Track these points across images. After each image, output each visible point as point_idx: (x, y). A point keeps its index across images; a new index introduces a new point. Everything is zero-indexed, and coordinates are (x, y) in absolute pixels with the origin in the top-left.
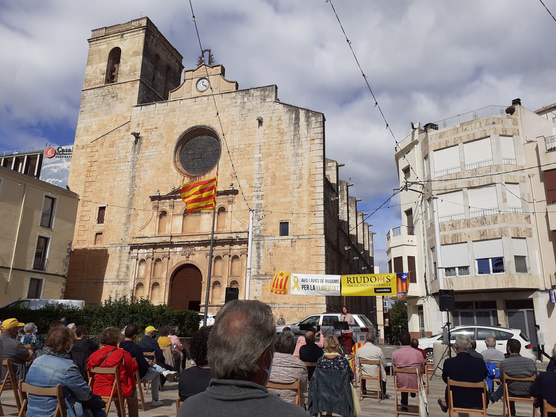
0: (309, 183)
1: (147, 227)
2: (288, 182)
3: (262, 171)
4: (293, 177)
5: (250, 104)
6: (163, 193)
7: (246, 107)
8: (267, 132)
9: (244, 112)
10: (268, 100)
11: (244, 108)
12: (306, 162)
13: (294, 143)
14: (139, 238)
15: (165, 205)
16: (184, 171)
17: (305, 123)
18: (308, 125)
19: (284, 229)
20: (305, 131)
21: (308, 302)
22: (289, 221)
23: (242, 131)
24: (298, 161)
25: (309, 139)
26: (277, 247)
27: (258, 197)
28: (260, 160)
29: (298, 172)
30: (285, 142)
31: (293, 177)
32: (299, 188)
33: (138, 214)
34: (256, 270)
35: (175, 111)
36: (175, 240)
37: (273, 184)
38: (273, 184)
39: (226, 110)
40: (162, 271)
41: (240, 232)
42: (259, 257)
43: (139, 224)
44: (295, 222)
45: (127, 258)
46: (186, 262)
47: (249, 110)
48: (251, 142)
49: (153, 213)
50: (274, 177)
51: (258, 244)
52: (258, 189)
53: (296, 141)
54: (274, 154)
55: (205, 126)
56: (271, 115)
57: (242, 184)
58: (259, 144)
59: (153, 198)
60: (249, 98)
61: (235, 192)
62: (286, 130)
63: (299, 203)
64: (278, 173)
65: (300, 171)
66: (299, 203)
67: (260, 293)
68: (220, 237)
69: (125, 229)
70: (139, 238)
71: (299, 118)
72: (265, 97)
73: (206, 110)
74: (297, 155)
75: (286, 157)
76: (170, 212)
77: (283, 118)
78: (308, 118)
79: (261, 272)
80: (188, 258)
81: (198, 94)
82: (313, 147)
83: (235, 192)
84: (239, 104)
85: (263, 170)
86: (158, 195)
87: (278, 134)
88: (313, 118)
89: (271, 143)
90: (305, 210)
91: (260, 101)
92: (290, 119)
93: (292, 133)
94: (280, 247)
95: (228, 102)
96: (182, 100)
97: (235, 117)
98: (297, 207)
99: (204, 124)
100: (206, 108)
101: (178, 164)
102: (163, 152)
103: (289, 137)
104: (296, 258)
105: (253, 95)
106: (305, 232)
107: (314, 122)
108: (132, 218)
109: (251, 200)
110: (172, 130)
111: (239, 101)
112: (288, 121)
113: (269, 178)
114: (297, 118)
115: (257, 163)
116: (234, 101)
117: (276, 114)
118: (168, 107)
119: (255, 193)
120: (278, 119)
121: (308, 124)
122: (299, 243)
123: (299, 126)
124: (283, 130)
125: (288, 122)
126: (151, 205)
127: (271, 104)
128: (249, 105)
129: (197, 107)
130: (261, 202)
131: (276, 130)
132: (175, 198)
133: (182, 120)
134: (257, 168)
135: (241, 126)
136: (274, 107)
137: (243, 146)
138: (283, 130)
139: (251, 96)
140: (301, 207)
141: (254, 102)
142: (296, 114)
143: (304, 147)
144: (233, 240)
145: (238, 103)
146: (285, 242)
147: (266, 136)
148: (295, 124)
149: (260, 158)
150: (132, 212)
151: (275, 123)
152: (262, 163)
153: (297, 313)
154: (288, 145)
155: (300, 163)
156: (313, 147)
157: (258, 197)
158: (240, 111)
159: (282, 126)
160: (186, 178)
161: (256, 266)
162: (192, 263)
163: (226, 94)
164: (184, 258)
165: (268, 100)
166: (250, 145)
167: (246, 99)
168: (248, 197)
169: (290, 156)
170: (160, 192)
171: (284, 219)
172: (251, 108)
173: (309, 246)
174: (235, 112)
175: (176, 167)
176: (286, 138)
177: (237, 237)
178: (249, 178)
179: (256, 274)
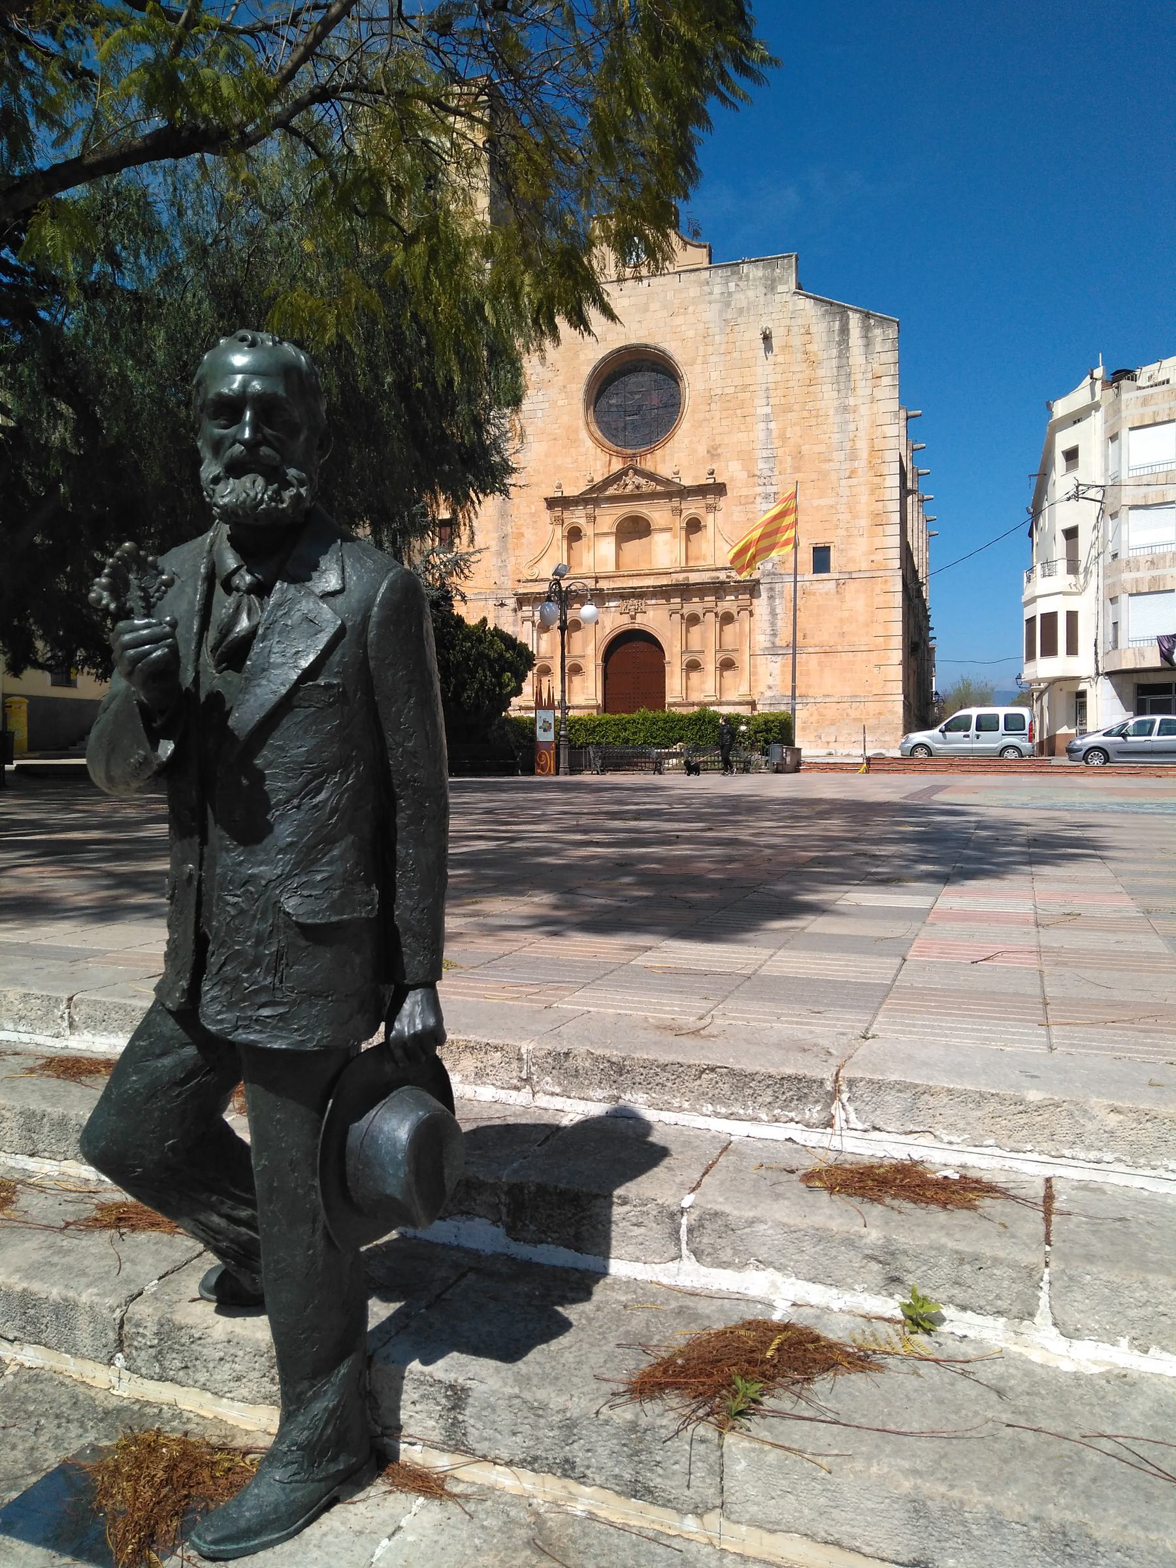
0: (872, 468)
1: (544, 559)
2: (826, 466)
3: (772, 443)
4: (838, 456)
5: (741, 296)
6: (571, 491)
7: (733, 303)
10: (780, 288)
11: (728, 305)
12: (864, 424)
14: (531, 581)
15: (577, 517)
16: (608, 443)
17: (861, 342)
18: (867, 346)
19: (821, 559)
20: (861, 359)
21: (870, 692)
22: (832, 545)
23: (728, 358)
24: (847, 422)
25: (870, 375)
27: (767, 497)
28: (767, 419)
30: (820, 381)
31: (838, 456)
32: (850, 477)
33: (522, 535)
34: (768, 638)
36: (604, 585)
37: (797, 469)
38: (797, 469)
39: (691, 309)
40: (585, 644)
42: (773, 613)
43: (526, 555)
44: (842, 547)
45: (511, 619)
46: (630, 627)
47: (741, 310)
48: (748, 381)
49: (554, 530)
50: (798, 455)
51: (772, 589)
53: (843, 379)
54: (796, 407)
55: (646, 346)
56: (788, 322)
57: (730, 472)
59: (552, 503)
61: (719, 489)
62: (822, 355)
64: (807, 447)
65: (851, 443)
67: (778, 679)
68: (694, 578)
69: (500, 564)
70: (531, 581)
72: (774, 281)
73: (646, 310)
74: (845, 409)
75: (821, 413)
76: (588, 530)
77: (813, 329)
78: (866, 329)
79: (778, 642)
80: (633, 617)
82: (879, 393)
83: (719, 489)
84: (718, 296)
85: (775, 441)
86: (560, 494)
87: (805, 365)
88: (877, 332)
89: (791, 384)
90: (864, 522)
91: (764, 291)
92: (830, 331)
93: (834, 363)
94: (814, 594)
95: (694, 291)
98: (847, 516)
99: (644, 341)
100: (647, 304)
101: (594, 428)
102: (560, 403)
103: (827, 370)
104: (846, 614)
105: (747, 275)
107: (879, 339)
108: (510, 539)
110: (576, 354)
111: (717, 290)
113: (789, 458)
114: (844, 330)
115: (762, 426)
116: (706, 288)
117: (800, 321)
119: (759, 489)
120: (803, 331)
122: (852, 586)
123: (848, 348)
124: (815, 355)
125: (825, 338)
126: (546, 516)
127: (787, 297)
128: (740, 300)
131: (800, 356)
132: (596, 502)
134: (762, 436)
135: (723, 347)
136: (795, 304)
140: (855, 517)
141: (751, 293)
142: (841, 321)
143: (860, 392)
144: (723, 583)
146: (823, 585)
147: (779, 369)
148: (839, 343)
151: (797, 341)
152: (772, 425)
153: (849, 711)
154: (827, 388)
155: (852, 427)
156: (879, 393)
158: (721, 312)
159: (813, 348)
160: (614, 459)
161: (768, 631)
162: (642, 627)
163: (688, 274)
164: (626, 619)
165: (780, 288)
166: (745, 387)
167: (732, 285)
168: (747, 496)
169: (831, 412)
170: (563, 488)
171: (821, 541)
172: (745, 305)
173: (872, 590)
174: (711, 313)
175: (591, 434)
176: (821, 372)
177: (728, 577)
178: (746, 458)
179: (769, 645)
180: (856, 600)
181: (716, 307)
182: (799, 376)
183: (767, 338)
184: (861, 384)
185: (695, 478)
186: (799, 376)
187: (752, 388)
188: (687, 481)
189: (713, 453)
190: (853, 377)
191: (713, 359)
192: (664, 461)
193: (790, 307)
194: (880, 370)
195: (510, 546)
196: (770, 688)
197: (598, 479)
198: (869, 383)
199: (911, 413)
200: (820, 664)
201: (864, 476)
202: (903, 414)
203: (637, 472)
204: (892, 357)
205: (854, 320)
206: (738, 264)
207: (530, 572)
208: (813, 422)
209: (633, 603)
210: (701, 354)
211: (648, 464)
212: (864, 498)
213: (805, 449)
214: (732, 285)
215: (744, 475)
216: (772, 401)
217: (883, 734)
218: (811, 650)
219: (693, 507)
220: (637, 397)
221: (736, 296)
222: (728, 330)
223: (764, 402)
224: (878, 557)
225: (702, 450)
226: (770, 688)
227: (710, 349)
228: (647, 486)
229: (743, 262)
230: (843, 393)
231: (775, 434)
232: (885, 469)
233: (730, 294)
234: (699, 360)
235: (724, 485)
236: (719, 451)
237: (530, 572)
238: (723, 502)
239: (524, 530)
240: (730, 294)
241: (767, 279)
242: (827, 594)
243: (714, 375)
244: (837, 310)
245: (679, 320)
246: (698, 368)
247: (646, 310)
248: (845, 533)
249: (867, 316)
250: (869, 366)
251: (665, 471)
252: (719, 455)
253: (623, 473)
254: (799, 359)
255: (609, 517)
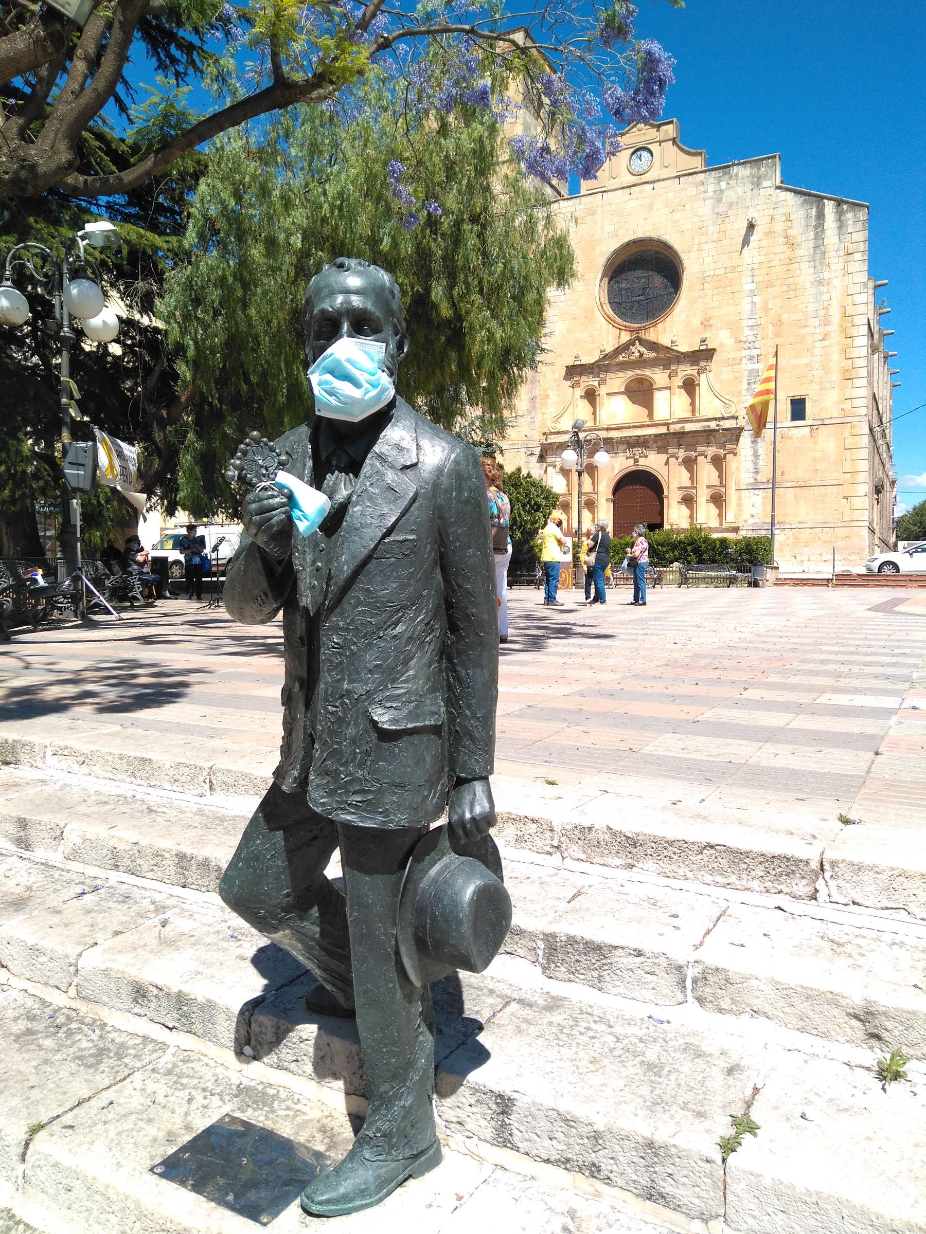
1: (565, 416)
2: (803, 331)
3: (756, 314)
7: (724, 199)
8: (764, 243)
9: (721, 208)
11: (720, 200)
13: (814, 261)
16: (618, 320)
18: (840, 228)
19: (798, 408)
20: (835, 239)
23: (719, 245)
24: (821, 293)
25: (842, 253)
26: (787, 438)
27: (751, 358)
28: (752, 294)
29: (821, 313)
30: (799, 260)
32: (823, 340)
33: (548, 396)
34: (751, 475)
35: (594, 213)
38: (777, 335)
39: (688, 207)
41: (723, 418)
42: (756, 455)
44: (815, 398)
46: (635, 468)
47: (731, 204)
50: (779, 323)
52: (751, 345)
53: (818, 257)
56: (771, 212)
57: (720, 339)
58: (750, 267)
60: (731, 182)
62: (800, 238)
63: (824, 367)
65: (824, 311)
66: (824, 367)
67: (760, 508)
71: (824, 215)
72: (759, 178)
73: (651, 209)
74: (820, 282)
75: (799, 286)
78: (840, 214)
79: (759, 478)
81: (635, 180)
82: (852, 267)
88: (850, 215)
89: (772, 264)
90: (836, 377)
91: (751, 186)
92: (808, 217)
93: (811, 244)
94: (791, 438)
95: (692, 191)
96: (605, 192)
97: (705, 218)
103: (805, 250)
104: (819, 454)
105: (737, 175)
106: (835, 414)
107: (850, 222)
108: (538, 400)
109: (739, 364)
111: (711, 188)
112: (803, 221)
113: (771, 326)
114: (821, 216)
115: (749, 299)
116: (702, 188)
118: (582, 206)
119: (746, 353)
120: (784, 218)
121: (841, 225)
123: (823, 230)
125: (803, 224)
127: (772, 191)
128: (730, 195)
129: (634, 203)
130: (756, 366)
131: (782, 240)
133: (610, 228)
136: (777, 196)
137: (722, 271)
138: (794, 237)
139: (734, 178)
141: (739, 190)
142: (818, 208)
143: (833, 267)
144: (714, 431)
145: (710, 193)
146: (799, 432)
147: (763, 251)
148: (816, 227)
149: (752, 291)
150: (537, 393)
151: (779, 227)
152: (756, 299)
154: (805, 265)
155: (826, 297)
156: (852, 267)
157: (751, 358)
158: (714, 207)
159: (792, 232)
161: (752, 469)
163: (686, 177)
165: (765, 184)
166: (733, 269)
167: (723, 184)
168: (734, 359)
169: (808, 285)
171: (797, 393)
172: (734, 199)
174: (705, 209)
176: (799, 252)
177: (718, 425)
178: (734, 327)
179: (752, 481)
180: (828, 441)
181: (710, 203)
182: (781, 256)
183: (751, 226)
184: (834, 260)
185: (690, 345)
186: (781, 256)
187: (739, 269)
188: (683, 348)
189: (706, 324)
190: (827, 255)
191: (705, 246)
192: (664, 332)
193: (774, 199)
194: (852, 248)
195: (537, 405)
196: (753, 516)
197: (609, 349)
198: (841, 259)
199: (879, 283)
200: (796, 496)
201: (836, 338)
202: (871, 284)
203: (642, 342)
204: (862, 236)
205: (829, 206)
206: (728, 167)
207: (553, 425)
208: (792, 294)
209: (637, 451)
210: (696, 242)
211: (651, 335)
212: (836, 357)
213: (785, 317)
214: (723, 184)
215: (731, 341)
216: (756, 279)
217: (850, 554)
218: (788, 485)
219: (686, 370)
220: (642, 281)
221: (727, 193)
222: (720, 221)
223: (750, 280)
224: (847, 406)
225: (696, 322)
226: (753, 516)
227: (704, 238)
228: (649, 355)
229: (734, 165)
230: (819, 268)
231: (759, 306)
232: (854, 332)
233: (722, 191)
234: (695, 248)
235: (714, 350)
236: (711, 322)
237: (553, 425)
238: (715, 364)
239: (550, 392)
240: (722, 191)
241: (754, 176)
242: (802, 438)
243: (707, 260)
244: (814, 199)
245: (678, 216)
246: (694, 255)
247: (651, 209)
248: (819, 387)
249: (839, 203)
250: (842, 245)
251: (665, 341)
252: (710, 326)
253: (631, 343)
254: (780, 243)
255: (617, 381)
